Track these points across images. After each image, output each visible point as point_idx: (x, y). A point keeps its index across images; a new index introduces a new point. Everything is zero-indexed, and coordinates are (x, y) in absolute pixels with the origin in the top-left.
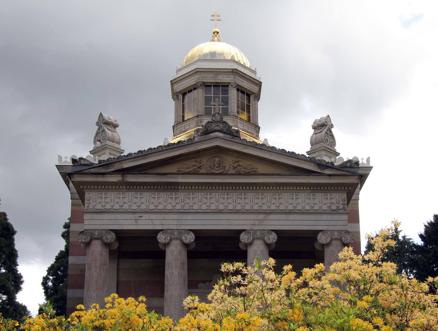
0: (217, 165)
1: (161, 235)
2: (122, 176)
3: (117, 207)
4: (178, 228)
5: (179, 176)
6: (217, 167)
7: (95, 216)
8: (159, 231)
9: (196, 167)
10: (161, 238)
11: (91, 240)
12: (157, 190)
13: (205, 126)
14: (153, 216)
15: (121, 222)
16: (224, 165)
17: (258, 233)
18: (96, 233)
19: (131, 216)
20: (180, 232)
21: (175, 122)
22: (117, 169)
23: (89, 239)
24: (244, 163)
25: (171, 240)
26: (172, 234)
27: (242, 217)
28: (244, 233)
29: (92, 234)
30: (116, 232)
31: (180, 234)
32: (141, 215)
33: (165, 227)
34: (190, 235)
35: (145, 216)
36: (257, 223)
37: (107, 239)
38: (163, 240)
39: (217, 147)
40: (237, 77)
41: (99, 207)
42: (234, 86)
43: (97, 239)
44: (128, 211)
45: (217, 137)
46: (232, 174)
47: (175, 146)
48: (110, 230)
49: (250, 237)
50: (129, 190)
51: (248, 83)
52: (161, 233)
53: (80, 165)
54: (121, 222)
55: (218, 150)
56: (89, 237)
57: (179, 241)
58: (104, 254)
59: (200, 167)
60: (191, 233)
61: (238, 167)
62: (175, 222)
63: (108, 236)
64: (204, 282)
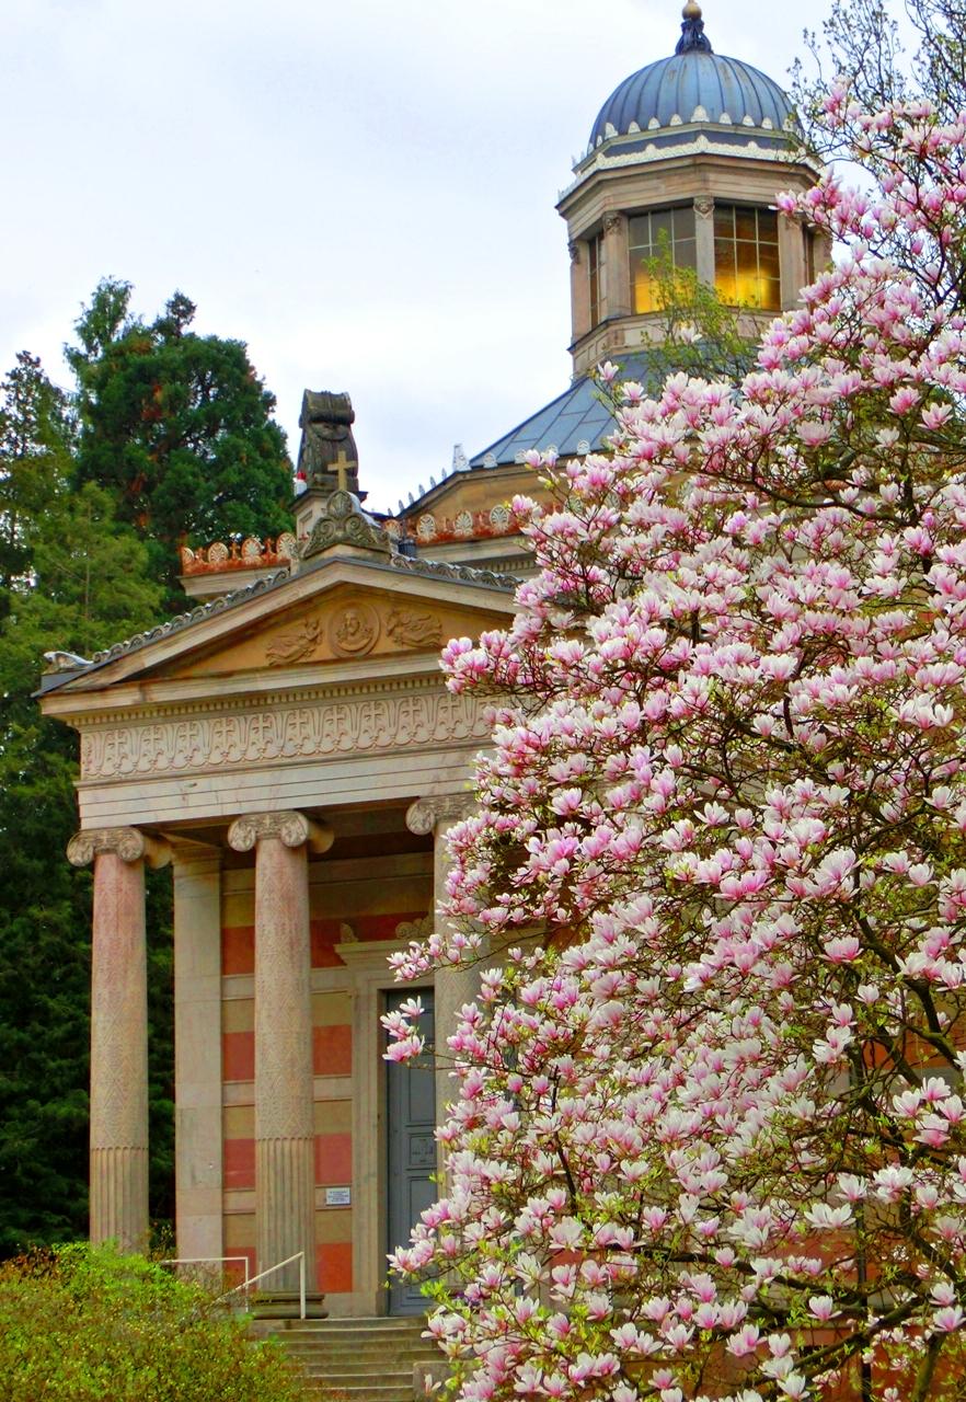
0: (351, 630)
1: (237, 830)
2: (141, 691)
3: (144, 765)
4: (273, 806)
5: (258, 675)
6: (353, 634)
7: (101, 793)
8: (234, 817)
9: (303, 642)
10: (238, 839)
11: (95, 855)
12: (222, 713)
13: (314, 532)
14: (217, 782)
15: (154, 804)
16: (368, 626)
17: (447, 804)
18: (105, 837)
19: (171, 787)
20: (277, 816)
21: (574, 334)
22: (130, 673)
23: (91, 854)
24: (410, 615)
25: (258, 840)
26: (260, 823)
27: (411, 762)
28: (415, 806)
29: (98, 840)
30: (144, 829)
31: (276, 821)
32: (192, 782)
33: (244, 809)
34: (298, 825)
35: (203, 783)
36: (444, 775)
37: (126, 850)
38: (241, 842)
39: (342, 585)
40: (712, 176)
41: (108, 769)
42: (704, 207)
43: (108, 851)
44: (167, 773)
45: (335, 561)
46: (386, 655)
47: (251, 596)
48: (134, 826)
49: (429, 815)
50: (167, 719)
51: (757, 181)
52: (236, 823)
53: (56, 673)
54: (154, 804)
55: (344, 593)
56: (91, 849)
57: (275, 841)
58: (125, 886)
59: (314, 640)
60: (302, 818)
61: (398, 630)
62: (265, 793)
63: (129, 843)
64: (410, 917)
